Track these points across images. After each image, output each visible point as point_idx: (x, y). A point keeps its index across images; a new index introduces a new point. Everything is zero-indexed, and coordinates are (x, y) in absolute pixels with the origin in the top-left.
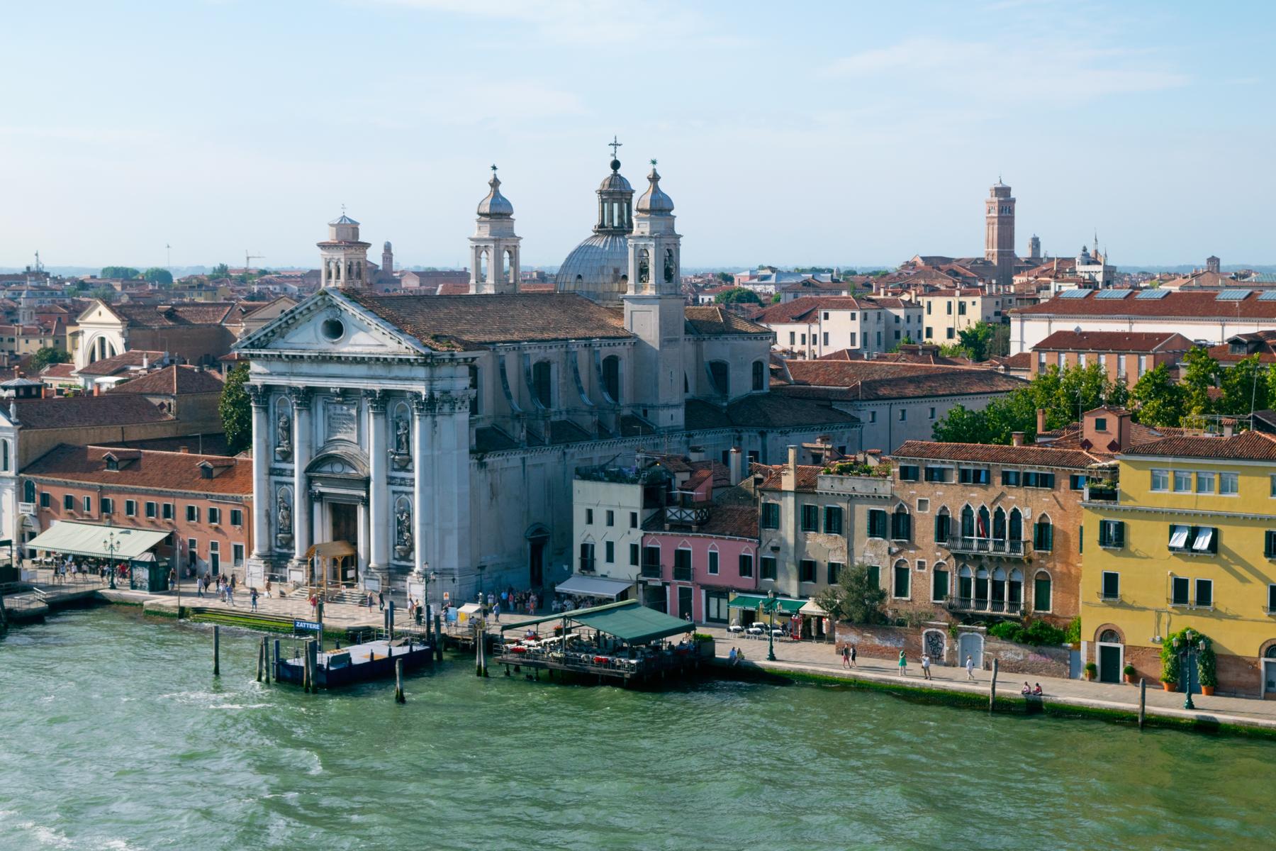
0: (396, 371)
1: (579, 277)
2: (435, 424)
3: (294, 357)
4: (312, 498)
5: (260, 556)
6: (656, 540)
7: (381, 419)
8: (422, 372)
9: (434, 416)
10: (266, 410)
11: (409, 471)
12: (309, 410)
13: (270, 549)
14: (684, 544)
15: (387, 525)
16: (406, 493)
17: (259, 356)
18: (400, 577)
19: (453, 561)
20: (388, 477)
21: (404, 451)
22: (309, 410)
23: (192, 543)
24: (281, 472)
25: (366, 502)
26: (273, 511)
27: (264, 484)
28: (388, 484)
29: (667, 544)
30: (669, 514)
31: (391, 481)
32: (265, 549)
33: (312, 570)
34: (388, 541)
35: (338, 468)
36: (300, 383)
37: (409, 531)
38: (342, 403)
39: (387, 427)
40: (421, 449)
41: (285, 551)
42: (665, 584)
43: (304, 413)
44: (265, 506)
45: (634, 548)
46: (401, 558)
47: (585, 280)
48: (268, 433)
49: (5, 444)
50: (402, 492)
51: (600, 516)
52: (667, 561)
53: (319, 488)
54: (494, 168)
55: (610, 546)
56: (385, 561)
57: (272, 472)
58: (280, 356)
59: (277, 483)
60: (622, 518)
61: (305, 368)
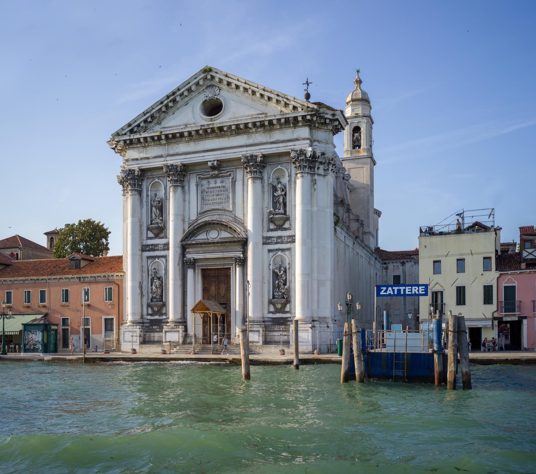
2: (314, 182)
4: (186, 264)
5: (135, 323)
7: (258, 182)
9: (313, 175)
10: (140, 193)
11: (286, 229)
12: (183, 187)
13: (142, 317)
15: (263, 282)
16: (283, 250)
18: (276, 328)
19: (327, 312)
20: (263, 238)
22: (183, 187)
23: (65, 321)
24: (154, 248)
25: (243, 262)
26: (145, 284)
27: (138, 258)
28: (264, 244)
31: (266, 241)
32: (138, 318)
33: (186, 330)
34: (263, 297)
35: (213, 235)
36: (177, 161)
37: (285, 284)
38: (217, 177)
39: (263, 192)
40: (303, 203)
41: (157, 317)
43: (179, 190)
44: (139, 279)
46: (277, 311)
48: (141, 214)
50: (279, 250)
56: (260, 315)
57: (144, 248)
59: (148, 258)
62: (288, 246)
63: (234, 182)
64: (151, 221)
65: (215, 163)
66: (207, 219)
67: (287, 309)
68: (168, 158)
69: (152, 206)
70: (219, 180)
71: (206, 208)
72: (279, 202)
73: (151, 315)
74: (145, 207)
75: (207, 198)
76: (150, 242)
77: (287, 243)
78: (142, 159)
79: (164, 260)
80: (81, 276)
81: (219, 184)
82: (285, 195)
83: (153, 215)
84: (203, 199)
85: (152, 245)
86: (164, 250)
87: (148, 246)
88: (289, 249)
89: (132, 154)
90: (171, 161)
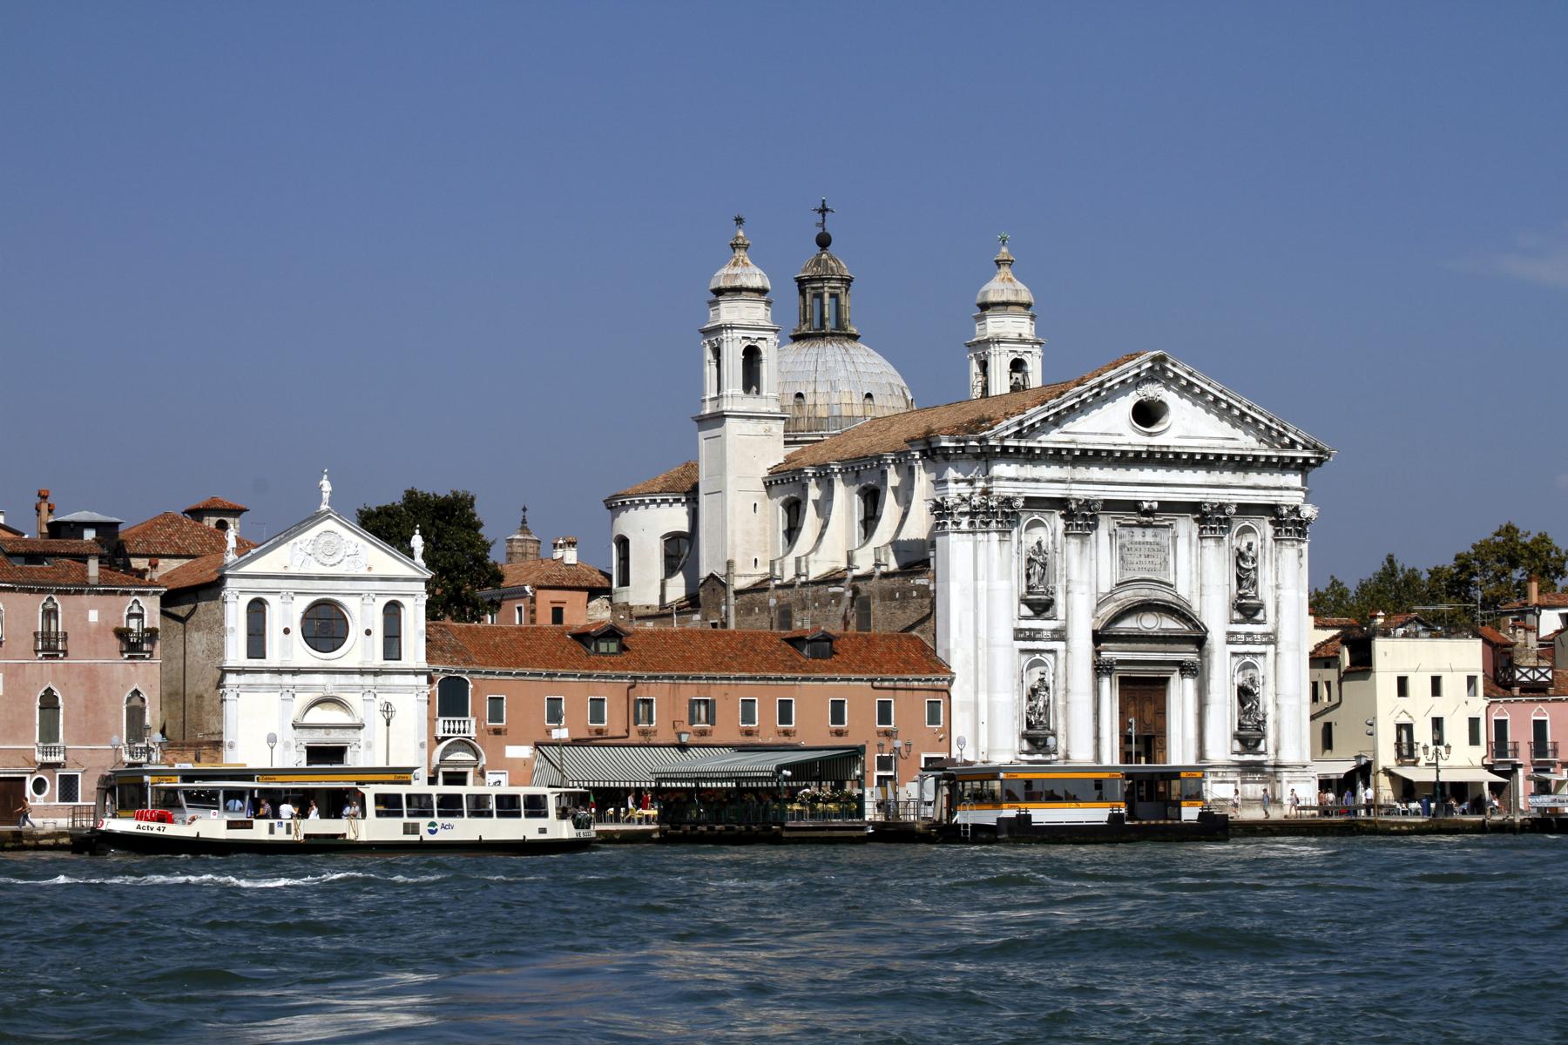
0: (1253, 478)
1: (869, 396)
3: (1097, 452)
4: (1101, 669)
6: (1502, 712)
8: (1294, 480)
11: (1259, 622)
14: (1540, 712)
16: (1254, 654)
17: (1031, 449)
18: (1249, 777)
21: (1252, 594)
24: (1033, 635)
29: (1521, 716)
30: (1518, 675)
31: (1231, 638)
35: (1150, 623)
38: (1149, 525)
41: (1039, 757)
42: (1515, 767)
45: (1474, 722)
47: (877, 400)
49: (393, 611)
51: (1419, 685)
52: (1520, 736)
53: (1112, 653)
54: (739, 221)
55: (1437, 723)
57: (1019, 634)
58: (1070, 451)
59: (1023, 651)
60: (1454, 685)
61: (1095, 473)
62: (1261, 649)
63: (1175, 538)
64: (1029, 587)
65: (1155, 505)
66: (1130, 595)
67: (1261, 747)
68: (1074, 486)
69: (1030, 560)
70: (1149, 532)
71: (1128, 576)
72: (1247, 579)
73: (1028, 753)
74: (1015, 561)
75: (1130, 559)
76: (1025, 624)
77: (1262, 643)
78: (1025, 480)
79: (1051, 657)
80: (879, 677)
81: (1149, 538)
82: (1255, 569)
83: (1034, 580)
84: (1122, 558)
85: (1030, 630)
86: (1053, 640)
87: (1021, 630)
88: (1263, 654)
89: (1000, 469)
90: (1079, 492)
